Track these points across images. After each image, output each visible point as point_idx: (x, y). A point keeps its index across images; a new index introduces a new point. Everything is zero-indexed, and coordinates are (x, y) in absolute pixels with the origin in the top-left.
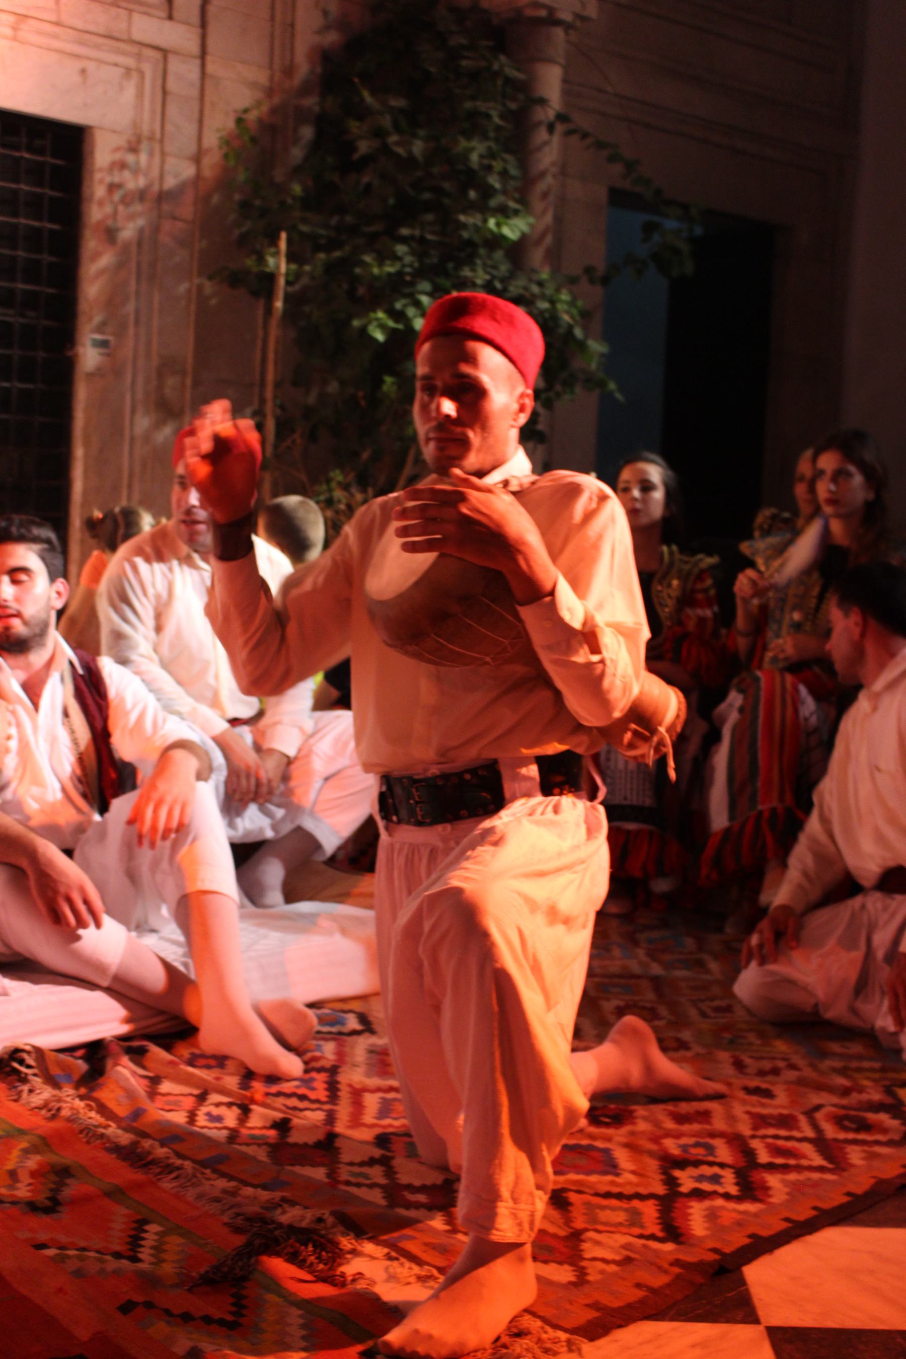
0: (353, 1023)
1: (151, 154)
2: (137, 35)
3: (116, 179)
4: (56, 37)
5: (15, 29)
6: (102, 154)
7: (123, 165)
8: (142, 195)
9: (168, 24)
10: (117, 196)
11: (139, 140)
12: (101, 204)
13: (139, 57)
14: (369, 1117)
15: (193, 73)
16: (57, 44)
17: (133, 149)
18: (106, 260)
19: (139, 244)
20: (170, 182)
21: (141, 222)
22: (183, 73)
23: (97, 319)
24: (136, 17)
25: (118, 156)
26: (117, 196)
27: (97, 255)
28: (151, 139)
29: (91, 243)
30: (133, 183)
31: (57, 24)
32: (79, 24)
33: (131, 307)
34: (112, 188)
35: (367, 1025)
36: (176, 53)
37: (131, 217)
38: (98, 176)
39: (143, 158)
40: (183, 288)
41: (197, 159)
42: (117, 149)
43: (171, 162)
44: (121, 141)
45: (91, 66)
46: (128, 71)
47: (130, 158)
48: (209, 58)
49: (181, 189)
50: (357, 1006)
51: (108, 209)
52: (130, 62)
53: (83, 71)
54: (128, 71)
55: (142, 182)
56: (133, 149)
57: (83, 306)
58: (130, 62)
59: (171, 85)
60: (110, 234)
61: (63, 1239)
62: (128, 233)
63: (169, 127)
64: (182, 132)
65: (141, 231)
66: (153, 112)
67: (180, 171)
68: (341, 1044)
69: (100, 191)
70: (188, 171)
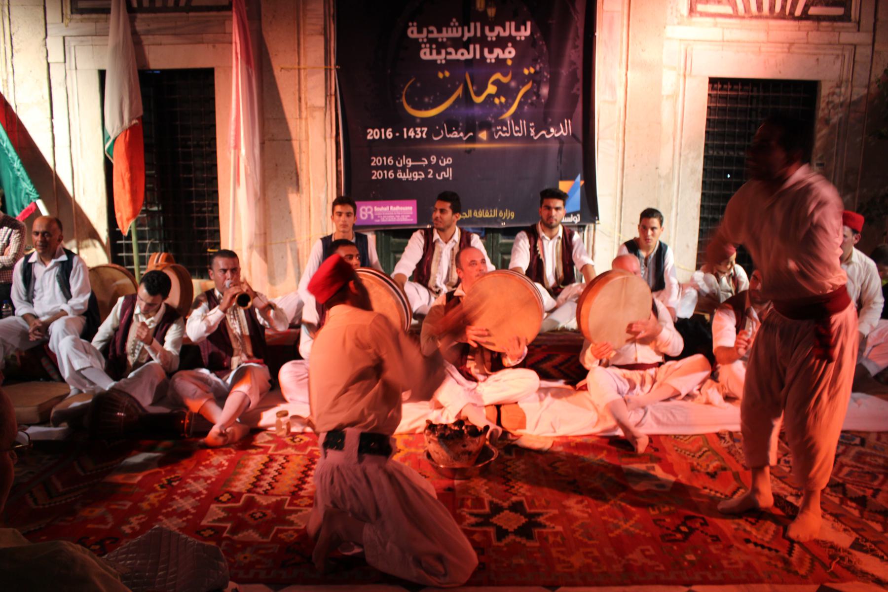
0: (857, 441)
1: (847, 88)
2: (842, 40)
3: (830, 99)
4: (807, 48)
5: (789, 49)
6: (824, 91)
7: (833, 94)
8: (841, 104)
9: (857, 34)
10: (830, 106)
11: (841, 82)
12: (823, 110)
13: (843, 50)
14: (841, 475)
15: (869, 52)
16: (806, 51)
17: (839, 86)
18: (824, 131)
19: (839, 124)
20: (855, 97)
21: (840, 115)
22: (864, 52)
23: (819, 156)
24: (842, 34)
25: (831, 90)
26: (830, 106)
27: (820, 130)
28: (847, 81)
29: (818, 126)
30: (837, 100)
31: (807, 43)
32: (816, 41)
33: (834, 149)
34: (828, 103)
35: (863, 443)
36: (860, 45)
37: (837, 113)
38: (822, 100)
39: (843, 89)
40: (858, 140)
41: (868, 87)
42: (831, 87)
43: (855, 90)
44: (834, 84)
45: (821, 57)
46: (838, 56)
47: (837, 90)
48: (876, 45)
49: (860, 100)
50: (863, 435)
51: (826, 111)
52: (840, 52)
53: (818, 60)
54: (838, 56)
55: (842, 99)
56: (839, 86)
57: (814, 150)
58: (840, 52)
59: (857, 58)
60: (827, 122)
61: (712, 487)
62: (835, 120)
63: (855, 75)
64: (862, 75)
65: (841, 119)
66: (848, 70)
67: (860, 92)
68: (847, 447)
69: (823, 105)
70: (864, 92)
